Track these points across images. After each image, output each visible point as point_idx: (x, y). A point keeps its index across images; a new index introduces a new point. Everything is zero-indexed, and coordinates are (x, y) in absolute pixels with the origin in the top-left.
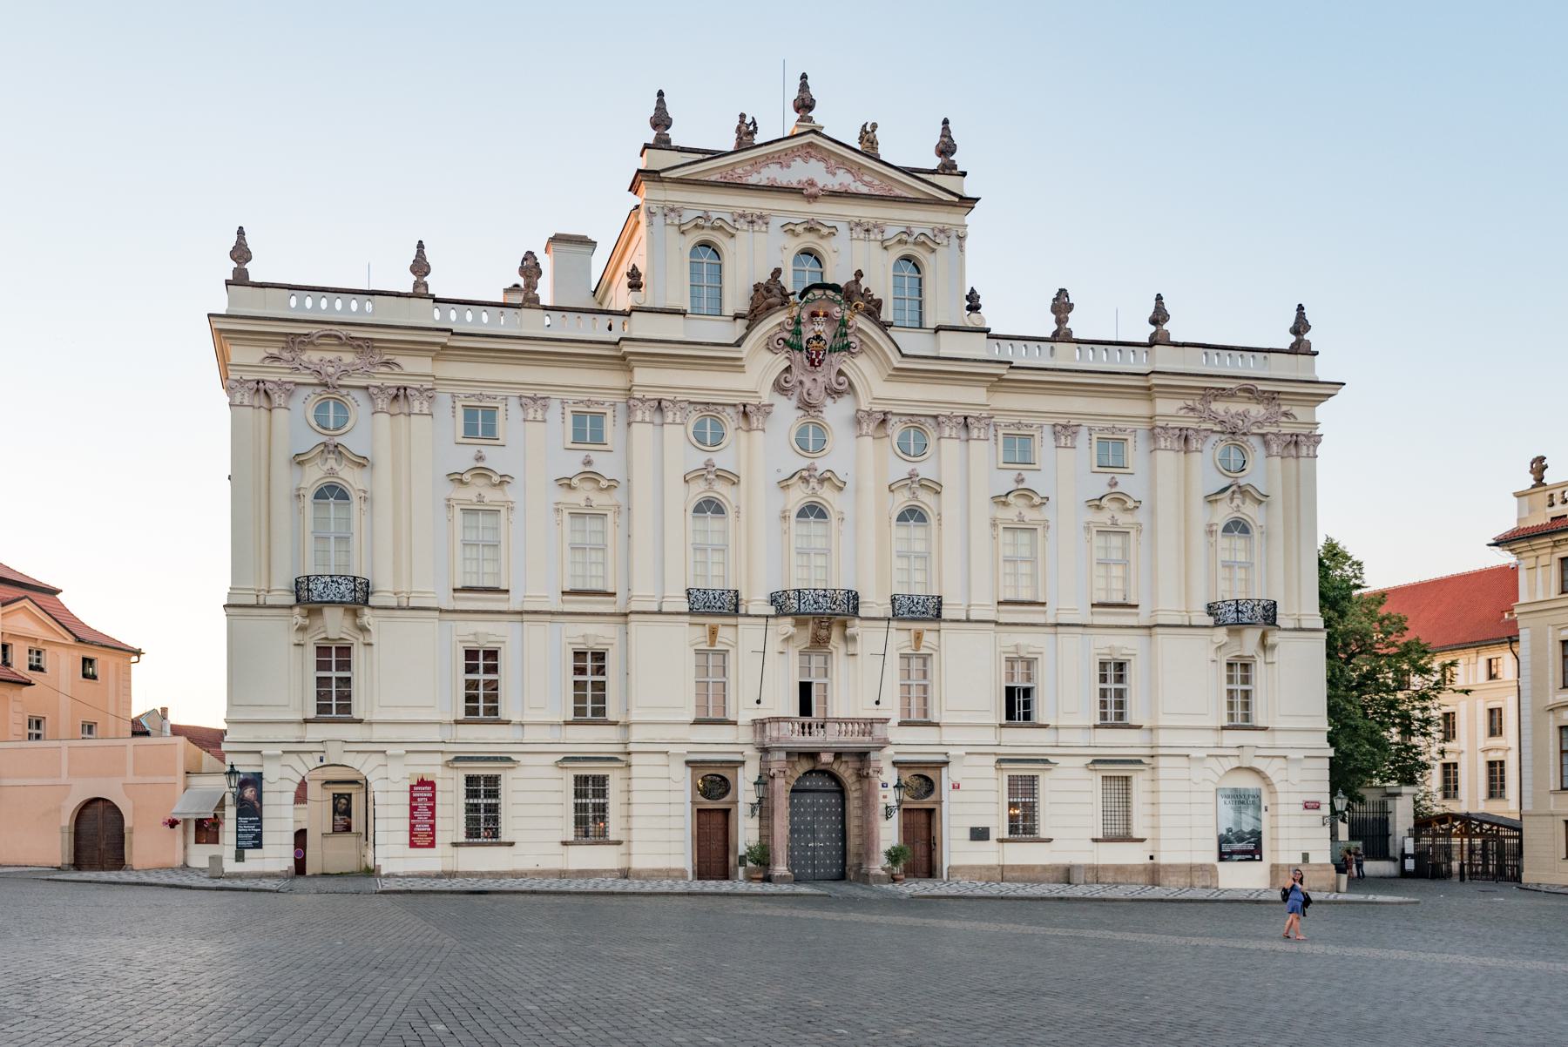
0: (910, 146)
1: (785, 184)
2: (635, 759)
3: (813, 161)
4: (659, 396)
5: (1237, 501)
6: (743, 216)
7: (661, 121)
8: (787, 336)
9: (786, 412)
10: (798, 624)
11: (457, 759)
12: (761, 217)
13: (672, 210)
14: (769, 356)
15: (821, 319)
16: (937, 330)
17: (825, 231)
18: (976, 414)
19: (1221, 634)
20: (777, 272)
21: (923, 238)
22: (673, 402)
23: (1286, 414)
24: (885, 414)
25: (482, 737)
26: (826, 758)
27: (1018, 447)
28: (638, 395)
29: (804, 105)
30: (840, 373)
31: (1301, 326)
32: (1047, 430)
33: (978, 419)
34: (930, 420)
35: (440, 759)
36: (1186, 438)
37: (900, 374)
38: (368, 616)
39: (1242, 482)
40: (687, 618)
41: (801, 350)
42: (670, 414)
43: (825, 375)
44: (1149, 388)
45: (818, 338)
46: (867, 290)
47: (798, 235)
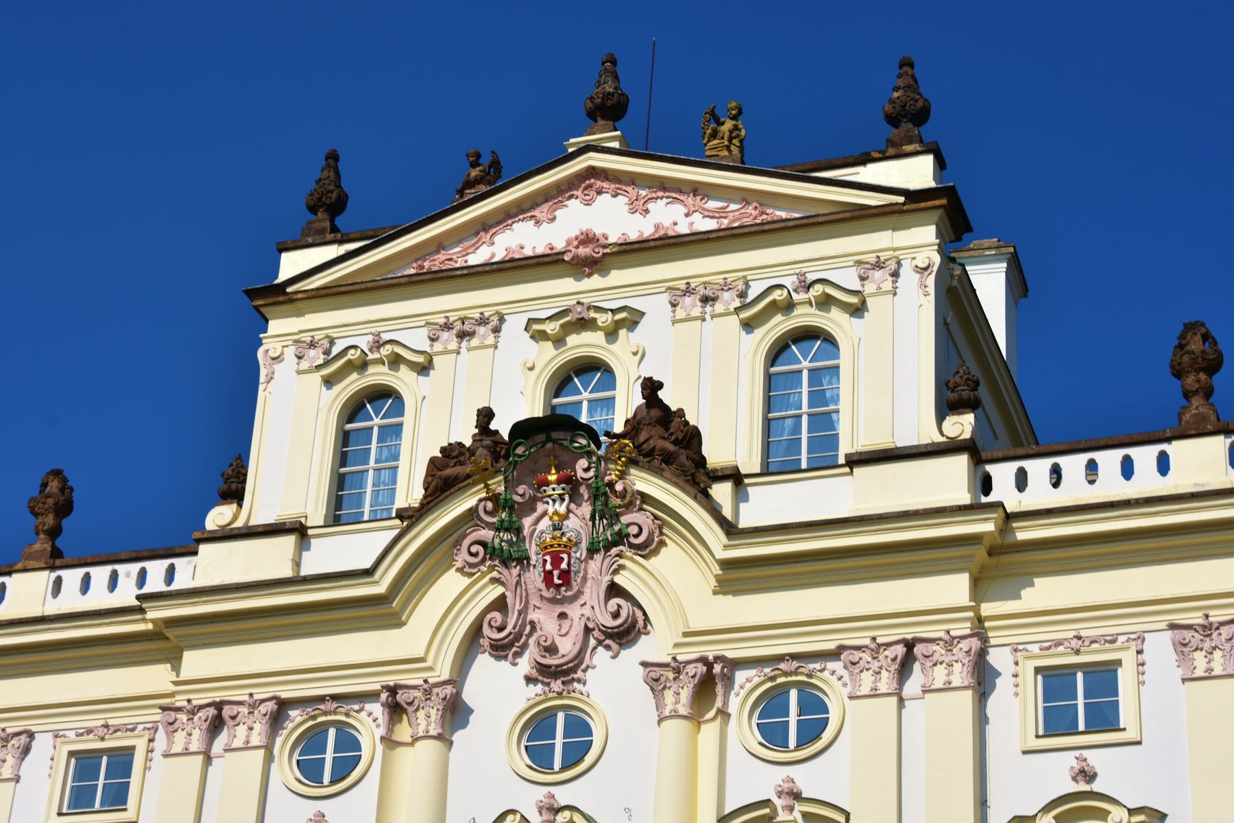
1: (540, 250)
3: (605, 198)
4: (217, 696)
6: (447, 327)
8: (487, 534)
9: (501, 692)
12: (483, 321)
13: (312, 345)
15: (554, 490)
16: (857, 461)
17: (603, 319)
18: (936, 632)
20: (486, 415)
21: (818, 289)
22: (254, 706)
27: (1081, 699)
28: (180, 701)
30: (614, 590)
32: (1160, 646)
33: (950, 643)
34: (831, 665)
42: (241, 731)
43: (590, 606)
45: (556, 528)
46: (681, 413)
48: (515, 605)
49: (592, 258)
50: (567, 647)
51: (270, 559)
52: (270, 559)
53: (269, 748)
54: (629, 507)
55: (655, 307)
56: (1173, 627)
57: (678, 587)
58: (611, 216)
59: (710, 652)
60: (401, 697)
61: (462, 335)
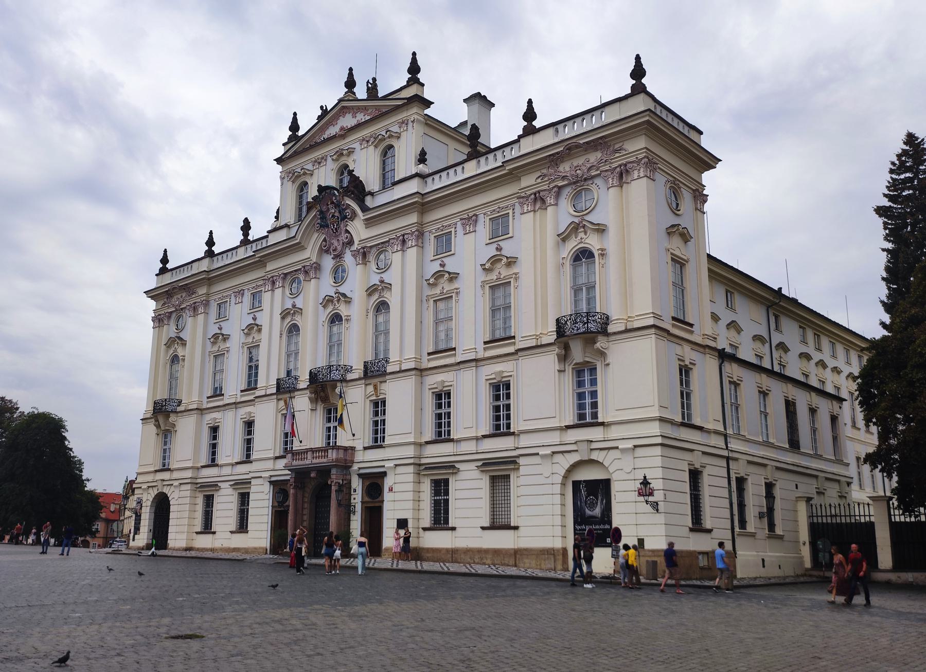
0: (393, 81)
2: (253, 482)
5: (582, 235)
6: (315, 161)
7: (294, 127)
9: (328, 262)
10: (315, 392)
11: (201, 487)
12: (322, 158)
14: (316, 235)
17: (345, 152)
19: (556, 350)
20: (319, 186)
23: (616, 151)
24: (363, 248)
25: (210, 474)
26: (313, 475)
29: (350, 84)
31: (638, 72)
32: (459, 224)
35: (188, 487)
36: (543, 201)
37: (369, 223)
38: (172, 418)
39: (586, 218)
40: (275, 397)
41: (327, 226)
43: (343, 237)
44: (511, 172)
47: (337, 160)
48: (328, 239)
49: (347, 132)
50: (339, 248)
51: (282, 236)
52: (282, 236)
53: (283, 287)
54: (345, 209)
55: (356, 145)
56: (461, 219)
57: (358, 230)
58: (348, 121)
59: (363, 245)
60: (307, 268)
61: (319, 163)
